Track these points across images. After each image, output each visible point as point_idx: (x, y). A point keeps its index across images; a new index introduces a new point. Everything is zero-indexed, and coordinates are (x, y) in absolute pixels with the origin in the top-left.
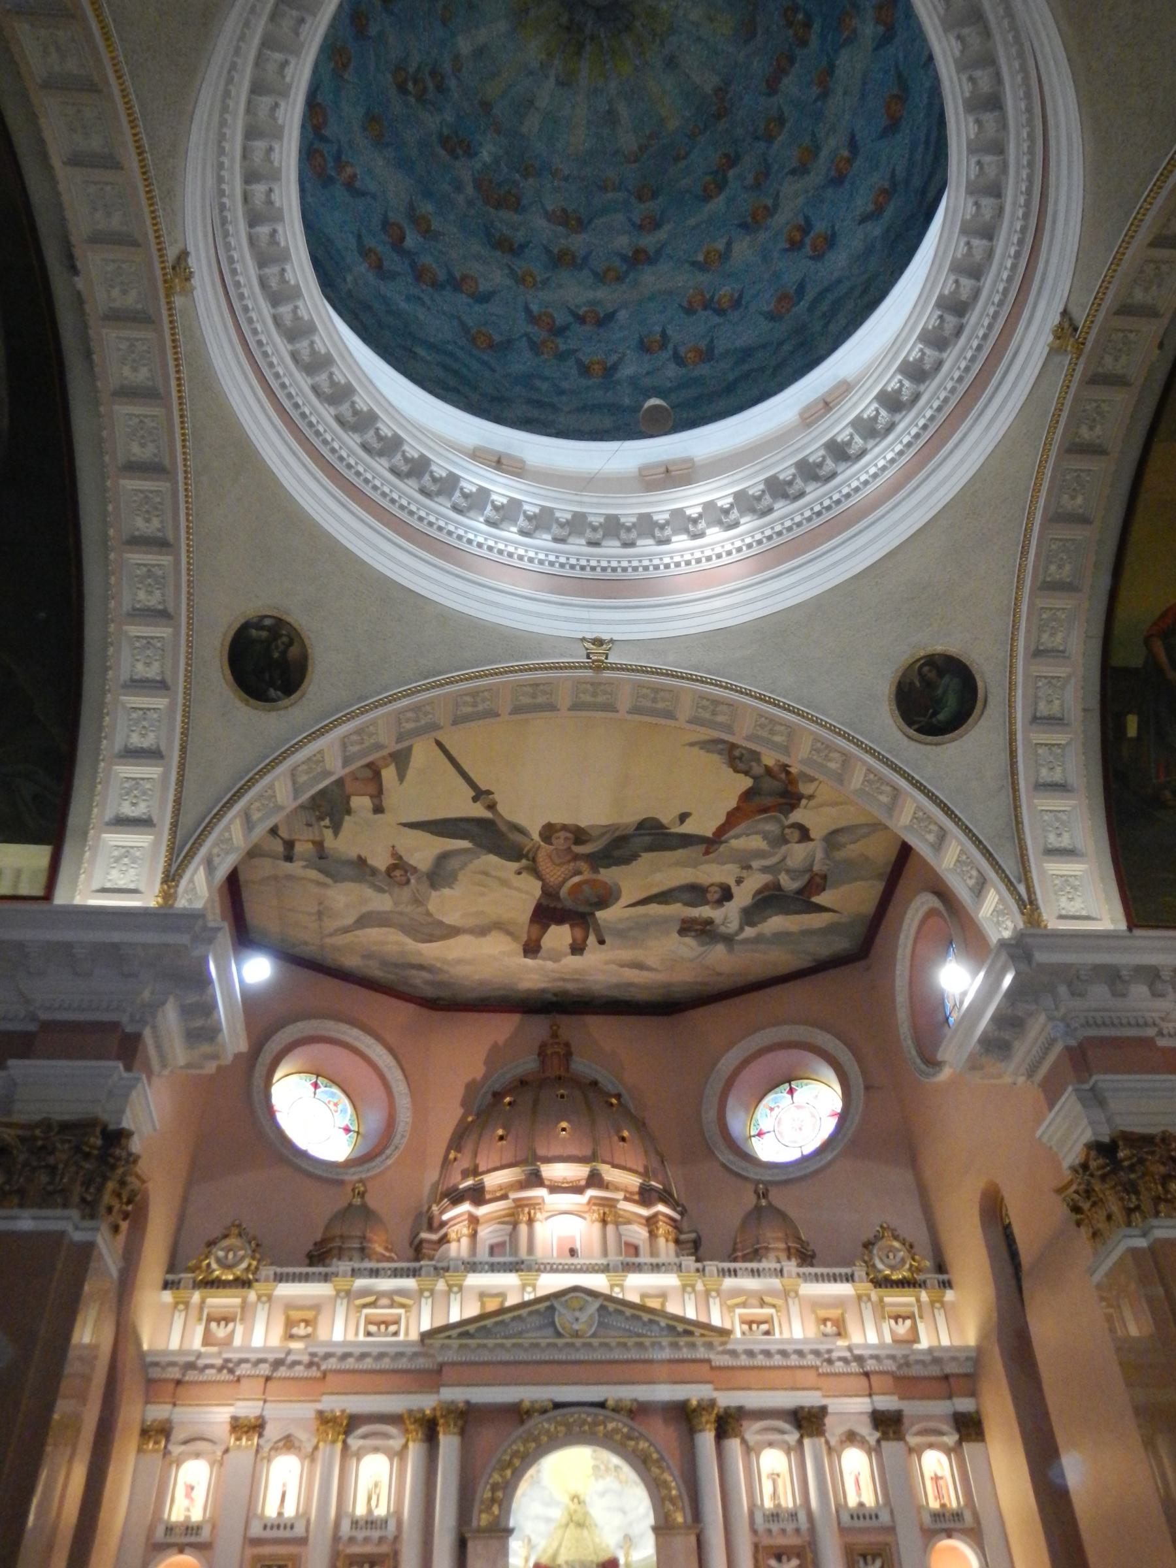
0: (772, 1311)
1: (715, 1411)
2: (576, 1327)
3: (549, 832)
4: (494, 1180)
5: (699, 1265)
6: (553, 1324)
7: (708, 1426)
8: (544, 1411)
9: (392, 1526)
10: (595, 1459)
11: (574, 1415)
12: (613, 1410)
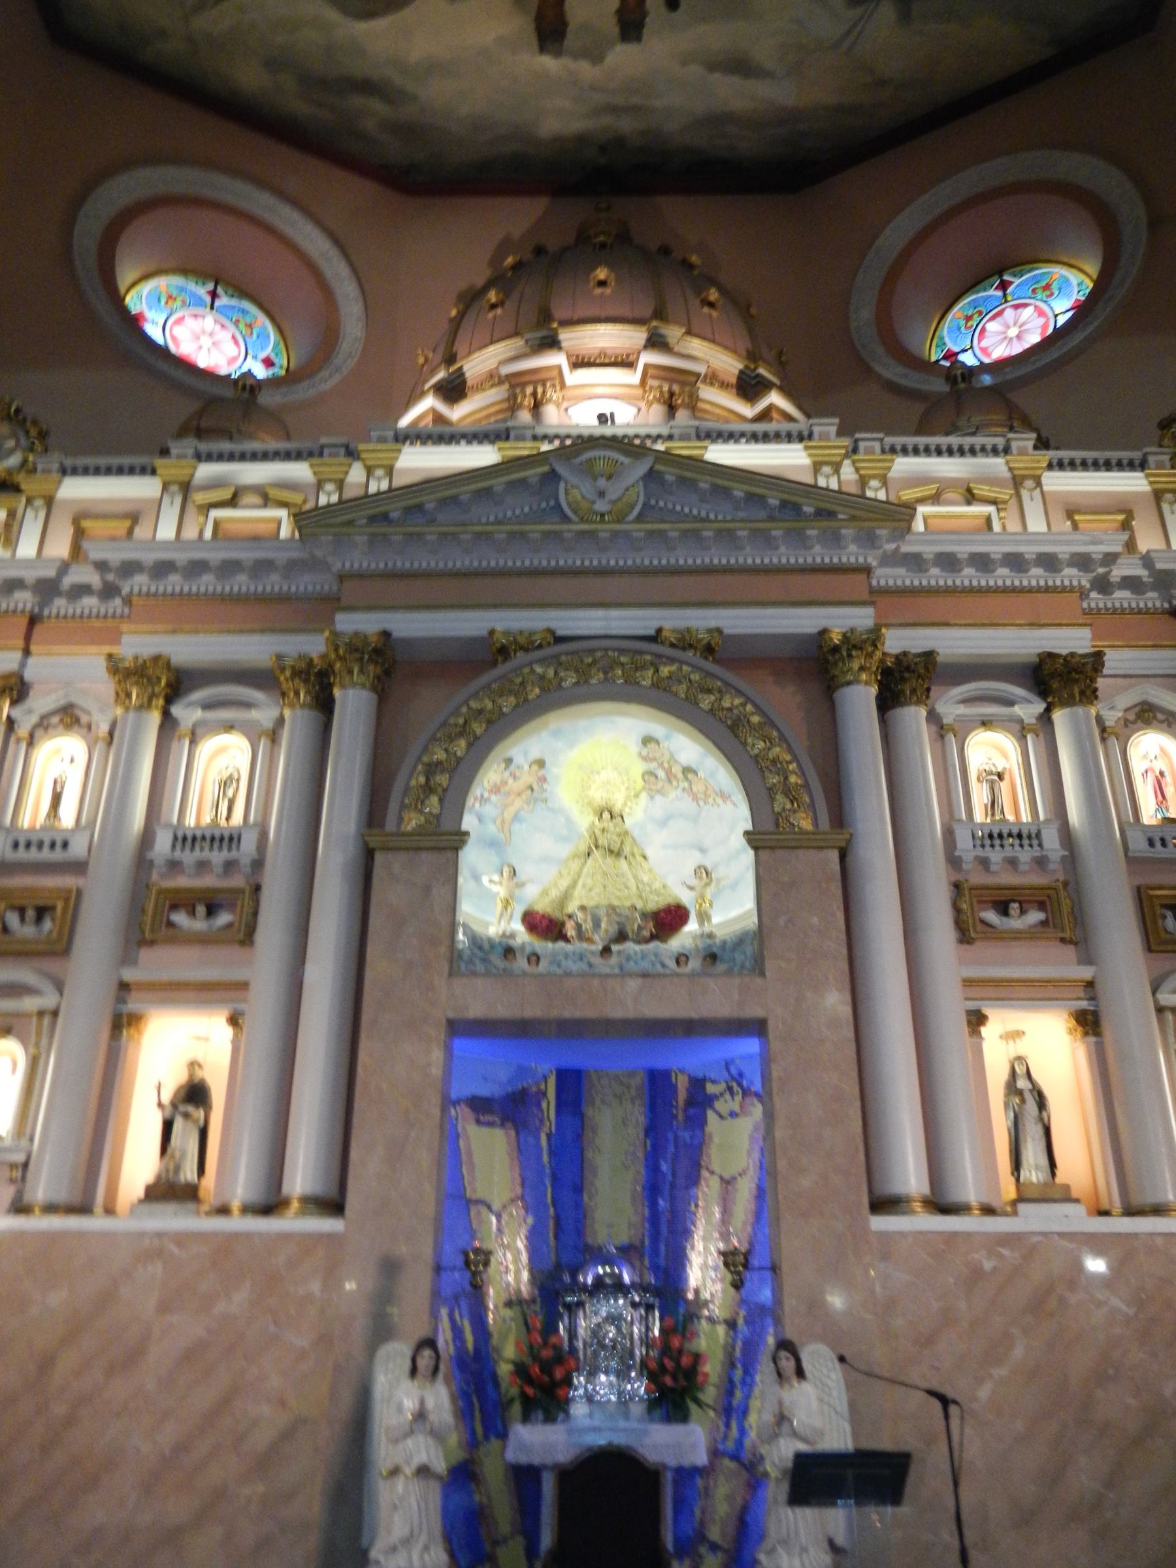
0: (991, 509)
1: (878, 654)
2: (601, 506)
5: (846, 442)
6: (558, 505)
7: (864, 677)
9: (249, 845)
10: (645, 759)
12: (672, 645)
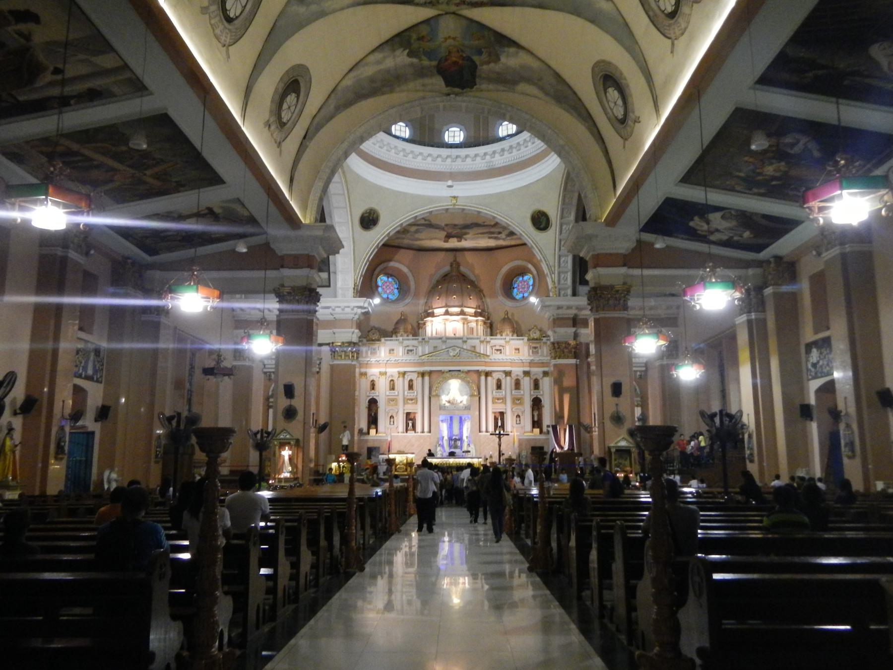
3: (447, 225)
4: (437, 311)
8: (447, 372)
11: (453, 373)
